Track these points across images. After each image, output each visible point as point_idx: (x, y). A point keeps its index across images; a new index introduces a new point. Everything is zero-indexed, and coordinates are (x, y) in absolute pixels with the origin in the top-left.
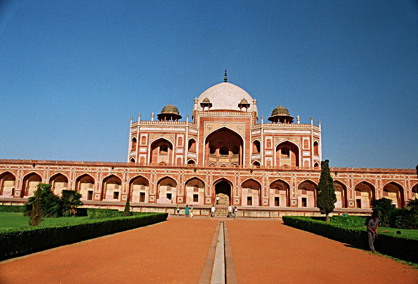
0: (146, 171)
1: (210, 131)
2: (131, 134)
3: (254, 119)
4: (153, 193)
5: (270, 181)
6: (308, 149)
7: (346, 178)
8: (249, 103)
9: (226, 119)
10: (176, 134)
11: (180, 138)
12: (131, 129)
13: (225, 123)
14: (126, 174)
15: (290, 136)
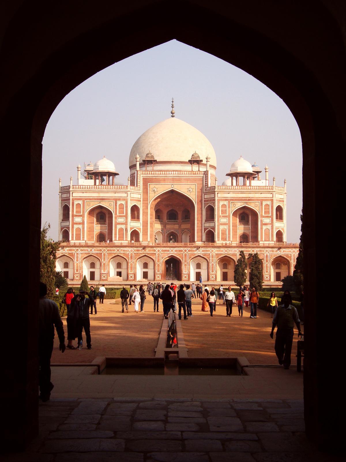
0: (98, 250)
1: (156, 194)
2: (61, 199)
3: (207, 180)
4: (104, 271)
5: (217, 258)
6: (268, 215)
7: (290, 253)
8: (201, 159)
9: (175, 180)
10: (116, 200)
11: (122, 204)
12: (60, 193)
13: (172, 184)
14: (78, 254)
15: (249, 200)
